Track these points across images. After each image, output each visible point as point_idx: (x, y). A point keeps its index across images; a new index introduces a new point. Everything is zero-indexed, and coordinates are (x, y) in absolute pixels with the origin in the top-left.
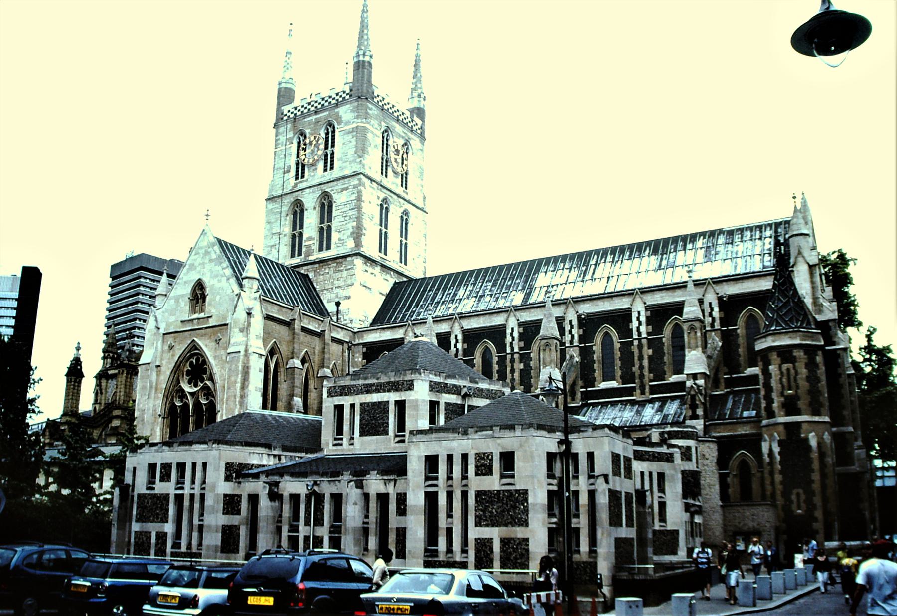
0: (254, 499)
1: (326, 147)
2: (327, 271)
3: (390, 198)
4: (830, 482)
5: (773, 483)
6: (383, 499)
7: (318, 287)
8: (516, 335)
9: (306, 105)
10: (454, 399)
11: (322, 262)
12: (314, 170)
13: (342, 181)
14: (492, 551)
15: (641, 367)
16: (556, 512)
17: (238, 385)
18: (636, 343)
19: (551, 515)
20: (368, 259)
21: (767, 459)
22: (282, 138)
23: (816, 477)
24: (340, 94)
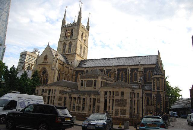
0: (65, 98)
4: (164, 103)
5: (154, 102)
6: (95, 100)
8: (105, 71)
10: (105, 81)
11: (69, 54)
14: (118, 111)
15: (129, 79)
16: (131, 104)
17: (53, 76)
19: (130, 105)
20: (78, 55)
21: (153, 98)
22: (63, 31)
23: (162, 101)
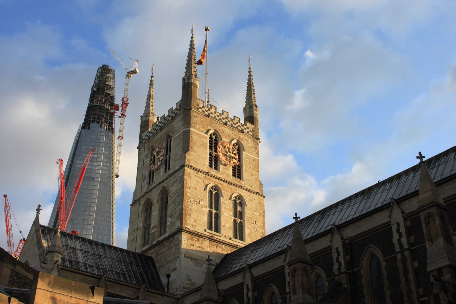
1: (167, 155)
2: (163, 251)
3: (219, 185)
7: (157, 266)
9: (155, 127)
11: (160, 243)
12: (158, 174)
13: (174, 176)
15: (408, 282)
18: (399, 256)
22: (142, 156)
24: (174, 112)
